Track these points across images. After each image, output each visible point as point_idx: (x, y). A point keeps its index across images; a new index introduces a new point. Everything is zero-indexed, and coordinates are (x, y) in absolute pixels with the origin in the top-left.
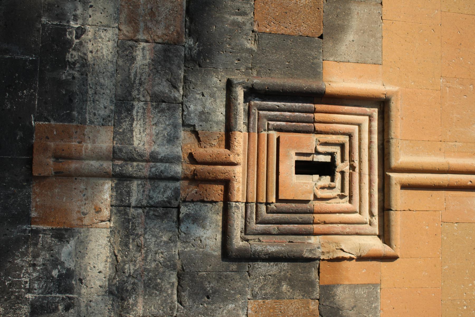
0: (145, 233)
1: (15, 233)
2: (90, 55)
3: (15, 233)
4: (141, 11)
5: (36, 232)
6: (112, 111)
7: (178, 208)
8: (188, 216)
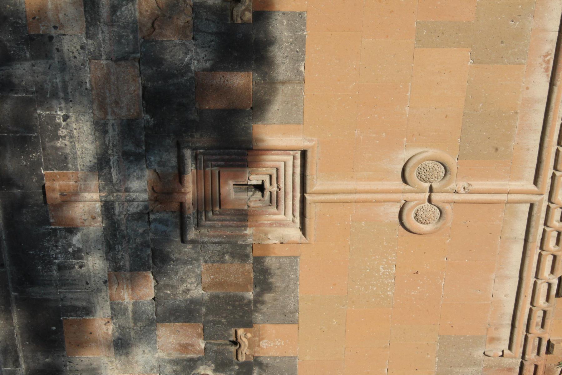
0: (127, 229)
1: (42, 230)
2: (75, 131)
3: (42, 230)
4: (108, 101)
5: (55, 230)
6: (95, 163)
7: (148, 213)
8: (155, 220)
